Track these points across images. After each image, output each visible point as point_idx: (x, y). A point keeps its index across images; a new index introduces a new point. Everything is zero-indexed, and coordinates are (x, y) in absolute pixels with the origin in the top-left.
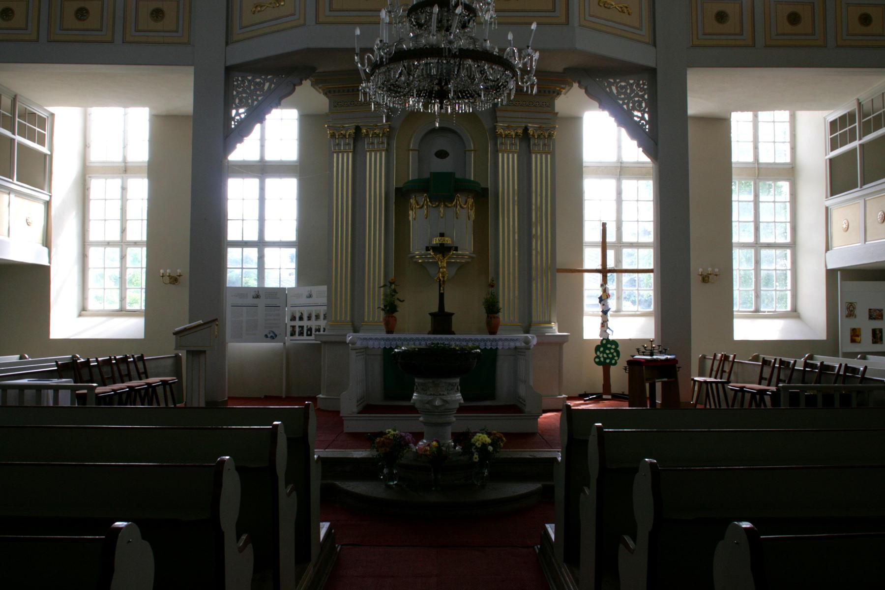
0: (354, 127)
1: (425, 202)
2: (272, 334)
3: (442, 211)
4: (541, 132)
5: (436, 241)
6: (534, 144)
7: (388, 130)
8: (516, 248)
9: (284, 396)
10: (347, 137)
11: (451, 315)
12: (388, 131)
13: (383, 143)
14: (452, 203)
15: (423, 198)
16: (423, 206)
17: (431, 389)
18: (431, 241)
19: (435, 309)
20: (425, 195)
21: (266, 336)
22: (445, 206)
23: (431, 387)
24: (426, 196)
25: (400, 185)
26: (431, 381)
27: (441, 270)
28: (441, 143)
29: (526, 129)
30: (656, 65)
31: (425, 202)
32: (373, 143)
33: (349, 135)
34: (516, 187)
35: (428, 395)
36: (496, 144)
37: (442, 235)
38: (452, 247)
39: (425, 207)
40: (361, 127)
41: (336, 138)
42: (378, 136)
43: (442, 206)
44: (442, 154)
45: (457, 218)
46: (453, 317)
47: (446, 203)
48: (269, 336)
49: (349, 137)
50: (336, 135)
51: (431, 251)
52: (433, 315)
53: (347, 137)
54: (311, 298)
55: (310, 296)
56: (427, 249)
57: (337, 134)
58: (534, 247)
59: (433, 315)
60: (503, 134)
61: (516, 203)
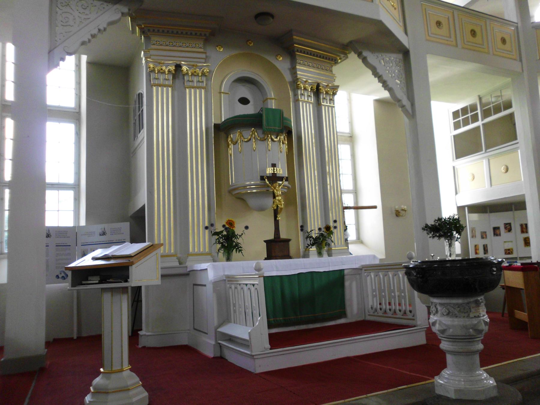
0: (175, 64)
1: (254, 136)
2: (63, 275)
3: (270, 145)
4: (329, 90)
5: (269, 171)
6: (324, 99)
7: (208, 71)
8: (317, 183)
9: (75, 337)
10: (167, 73)
11: (288, 241)
12: (208, 72)
13: (203, 82)
14: (277, 138)
15: (247, 133)
16: (250, 139)
17: (473, 310)
18: (265, 171)
19: (271, 236)
20: (253, 129)
21: (58, 277)
22: (272, 140)
23: (473, 308)
24: (254, 130)
25: (219, 122)
26: (472, 300)
27: (277, 198)
28: (244, 91)
29: (318, 85)
30: (409, 47)
31: (254, 136)
32: (192, 81)
33: (169, 71)
34: (313, 132)
35: (472, 318)
36: (295, 95)
37: (274, 165)
38: (283, 177)
39: (254, 140)
40: (181, 65)
41: (155, 72)
42: (198, 75)
43: (270, 140)
44: (244, 101)
45: (281, 152)
46: (290, 243)
47: (273, 137)
48: (60, 276)
49: (168, 74)
50: (155, 70)
51: (266, 180)
52: (268, 242)
53: (167, 73)
54: (104, 236)
55: (104, 234)
56: (262, 178)
57: (156, 70)
58: (328, 183)
59: (268, 242)
60: (302, 86)
61: (314, 145)
